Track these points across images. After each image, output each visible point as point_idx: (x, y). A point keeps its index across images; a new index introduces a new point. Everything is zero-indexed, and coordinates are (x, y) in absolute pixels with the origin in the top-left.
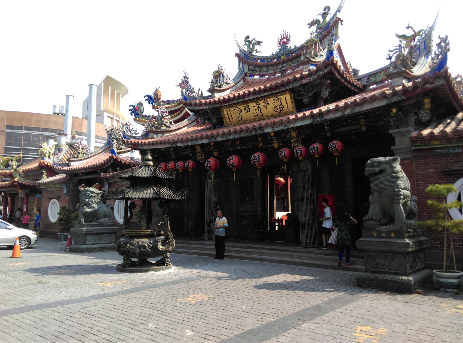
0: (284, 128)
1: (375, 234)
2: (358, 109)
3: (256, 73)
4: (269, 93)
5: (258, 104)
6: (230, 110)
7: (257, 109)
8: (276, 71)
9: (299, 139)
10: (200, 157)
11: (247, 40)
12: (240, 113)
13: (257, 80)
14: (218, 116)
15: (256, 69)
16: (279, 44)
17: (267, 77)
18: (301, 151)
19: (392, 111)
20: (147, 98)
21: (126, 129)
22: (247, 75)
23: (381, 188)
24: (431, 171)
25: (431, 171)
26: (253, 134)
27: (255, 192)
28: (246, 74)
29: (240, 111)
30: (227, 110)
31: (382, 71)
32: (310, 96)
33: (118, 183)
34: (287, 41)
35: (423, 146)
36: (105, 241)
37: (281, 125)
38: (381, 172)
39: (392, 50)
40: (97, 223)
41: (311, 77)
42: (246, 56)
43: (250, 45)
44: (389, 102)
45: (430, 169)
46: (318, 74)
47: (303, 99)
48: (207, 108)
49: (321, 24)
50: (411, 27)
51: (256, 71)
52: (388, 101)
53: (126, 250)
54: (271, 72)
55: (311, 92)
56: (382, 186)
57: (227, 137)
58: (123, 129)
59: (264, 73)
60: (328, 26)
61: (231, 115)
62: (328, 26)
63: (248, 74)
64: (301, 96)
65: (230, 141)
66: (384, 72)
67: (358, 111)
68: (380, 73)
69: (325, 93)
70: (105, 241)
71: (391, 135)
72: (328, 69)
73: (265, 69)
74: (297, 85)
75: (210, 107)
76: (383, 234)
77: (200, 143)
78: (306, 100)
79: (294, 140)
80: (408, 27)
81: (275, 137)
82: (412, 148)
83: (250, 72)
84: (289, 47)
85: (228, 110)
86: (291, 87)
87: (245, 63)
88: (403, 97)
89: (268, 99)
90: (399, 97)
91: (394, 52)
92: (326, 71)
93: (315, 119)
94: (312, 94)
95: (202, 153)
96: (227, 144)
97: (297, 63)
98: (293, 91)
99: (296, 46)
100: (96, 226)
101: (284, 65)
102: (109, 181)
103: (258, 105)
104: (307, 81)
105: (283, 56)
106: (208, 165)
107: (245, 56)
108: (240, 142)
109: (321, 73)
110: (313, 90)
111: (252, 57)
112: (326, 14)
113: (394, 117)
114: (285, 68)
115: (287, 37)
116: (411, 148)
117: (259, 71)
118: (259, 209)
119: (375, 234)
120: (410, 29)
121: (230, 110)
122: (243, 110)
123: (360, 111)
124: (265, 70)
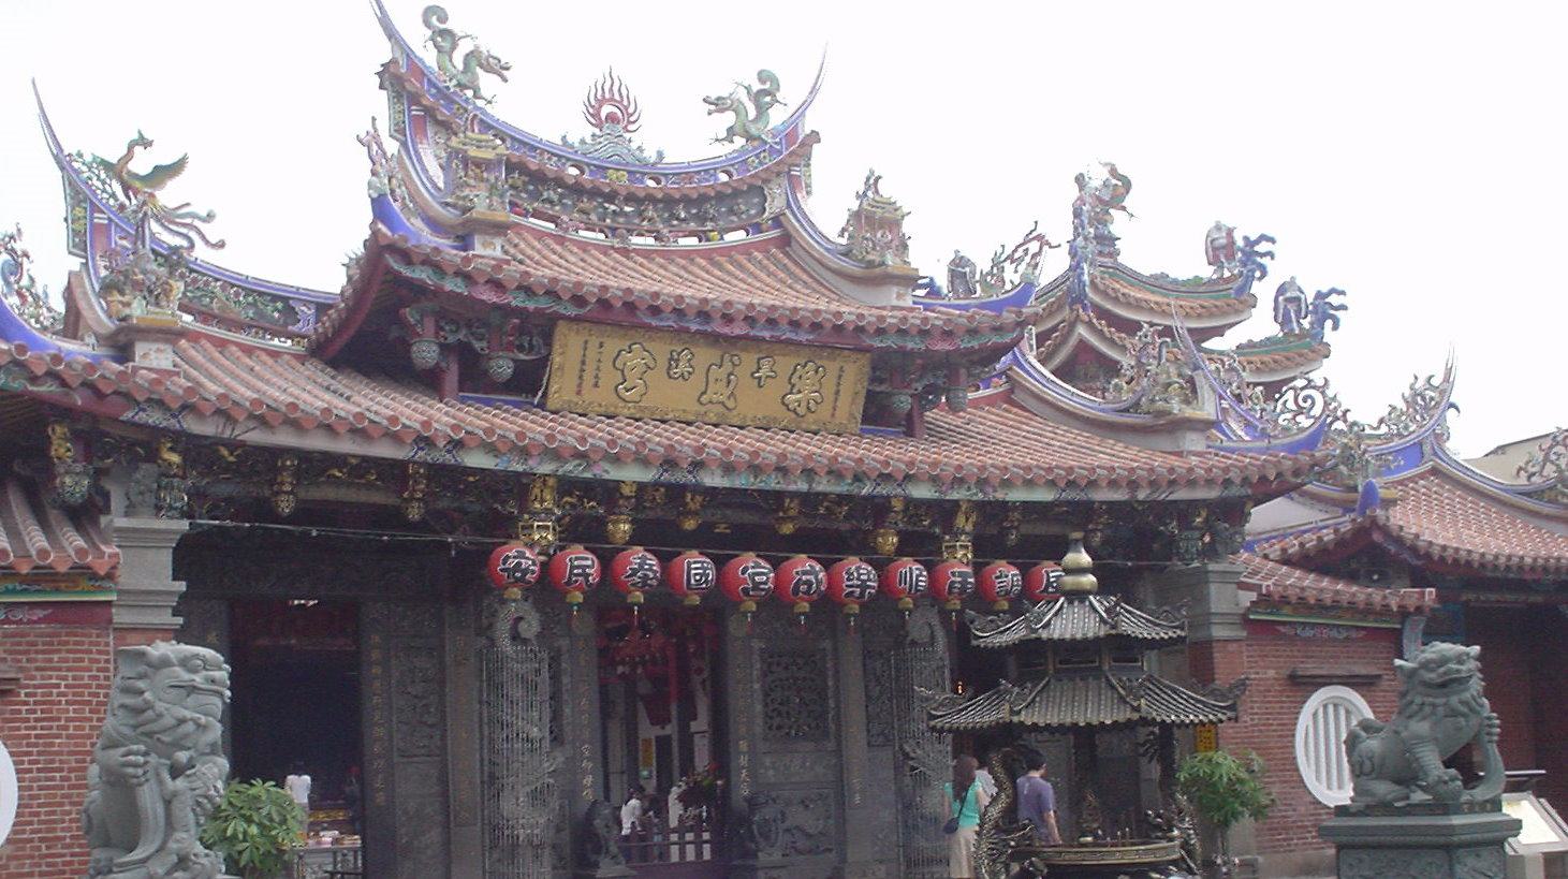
14: (521, 348)
24: (1271, 673)
25: (1271, 673)
26: (864, 492)
30: (586, 342)
35: (1269, 614)
45: (1269, 668)
47: (889, 395)
57: (752, 480)
61: (598, 369)
65: (662, 490)
76: (1477, 809)
77: (606, 477)
78: (904, 402)
79: (963, 538)
84: (634, 146)
85: (594, 342)
89: (779, 355)
99: (660, 155)
103: (734, 365)
121: (601, 346)
122: (662, 362)
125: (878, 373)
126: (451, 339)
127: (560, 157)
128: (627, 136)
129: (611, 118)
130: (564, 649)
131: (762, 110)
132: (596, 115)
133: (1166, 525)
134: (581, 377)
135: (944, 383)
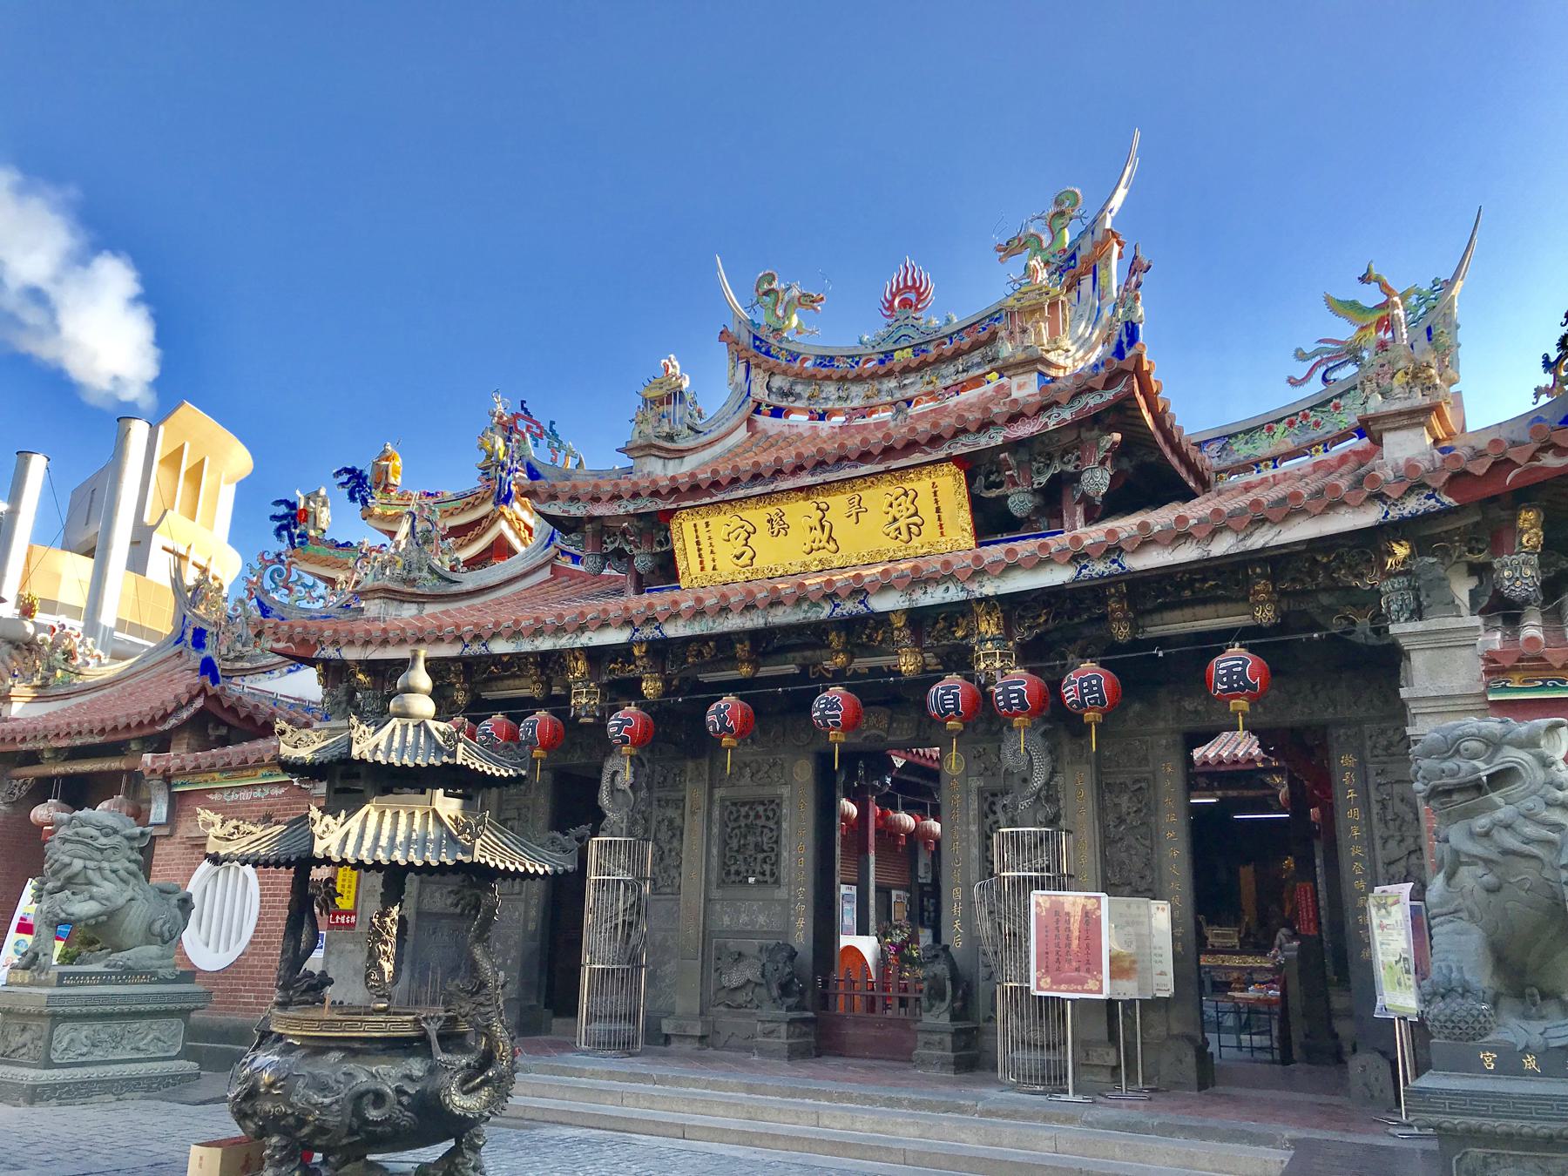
0: (956, 599)
1: (1489, 1059)
2: (1267, 538)
3: (797, 404)
4: (881, 468)
5: (823, 506)
6: (707, 524)
7: (818, 527)
8: (875, 401)
9: (1011, 644)
10: (584, 701)
11: (766, 287)
12: (746, 540)
13: (800, 430)
14: (661, 544)
15: (798, 389)
16: (887, 309)
17: (838, 420)
18: (1020, 692)
19: (1392, 554)
20: (345, 478)
21: (272, 579)
22: (763, 408)
23: (1506, 852)
26: (823, 616)
27: (785, 854)
28: (759, 404)
29: (751, 529)
30: (695, 525)
31: (1278, 421)
32: (1035, 486)
33: (211, 797)
34: (919, 301)
36: (138, 1049)
37: (945, 586)
38: (1501, 778)
39: (1308, 351)
40: (114, 966)
41: (1049, 417)
42: (761, 341)
43: (776, 304)
44: (1391, 513)
46: (1078, 406)
47: (1007, 497)
48: (621, 511)
49: (1046, 249)
50: (1378, 280)
51: (798, 397)
52: (1387, 513)
53: (285, 1115)
54: (857, 403)
55: (1039, 473)
56: (1511, 842)
57: (711, 624)
58: (261, 577)
59: (829, 405)
60: (1073, 257)
62: (1073, 257)
63: (767, 406)
64: (999, 485)
65: (711, 644)
66: (1282, 426)
67: (1267, 543)
68: (1270, 429)
69: (1098, 480)
70: (138, 1049)
71: (1395, 639)
72: (1119, 389)
73: (831, 390)
74: (993, 444)
75: (631, 509)
76: (1530, 1062)
78: (1019, 502)
79: (989, 645)
80: (1365, 279)
81: (907, 632)
82: (1491, 698)
83: (776, 401)
85: (701, 523)
86: (965, 450)
87: (758, 366)
88: (1448, 500)
90: (1429, 497)
91: (1318, 358)
92: (1109, 395)
93: (1085, 567)
94: (1044, 480)
95: (592, 685)
96: (700, 654)
97: (955, 378)
98: (970, 465)
100: (103, 983)
101: (906, 382)
102: (176, 785)
104: (1035, 429)
105: (902, 349)
106: (619, 732)
107: (758, 343)
108: (751, 647)
109: (1092, 403)
110: (1048, 466)
111: (781, 349)
112: (1067, 217)
113: (1400, 574)
114: (910, 393)
115: (918, 285)
116: (1484, 694)
117: (809, 399)
118: (801, 923)
119: (1489, 1059)
120: (1375, 285)
121: (707, 524)
122: (763, 527)
123: (1272, 543)
124: (833, 397)
125: (992, 478)
126: (611, 548)
127: (852, 357)
128: (917, 315)
129: (905, 303)
130: (786, 795)
131: (1055, 235)
132: (891, 307)
133: (1360, 576)
134: (700, 556)
135: (1076, 467)
